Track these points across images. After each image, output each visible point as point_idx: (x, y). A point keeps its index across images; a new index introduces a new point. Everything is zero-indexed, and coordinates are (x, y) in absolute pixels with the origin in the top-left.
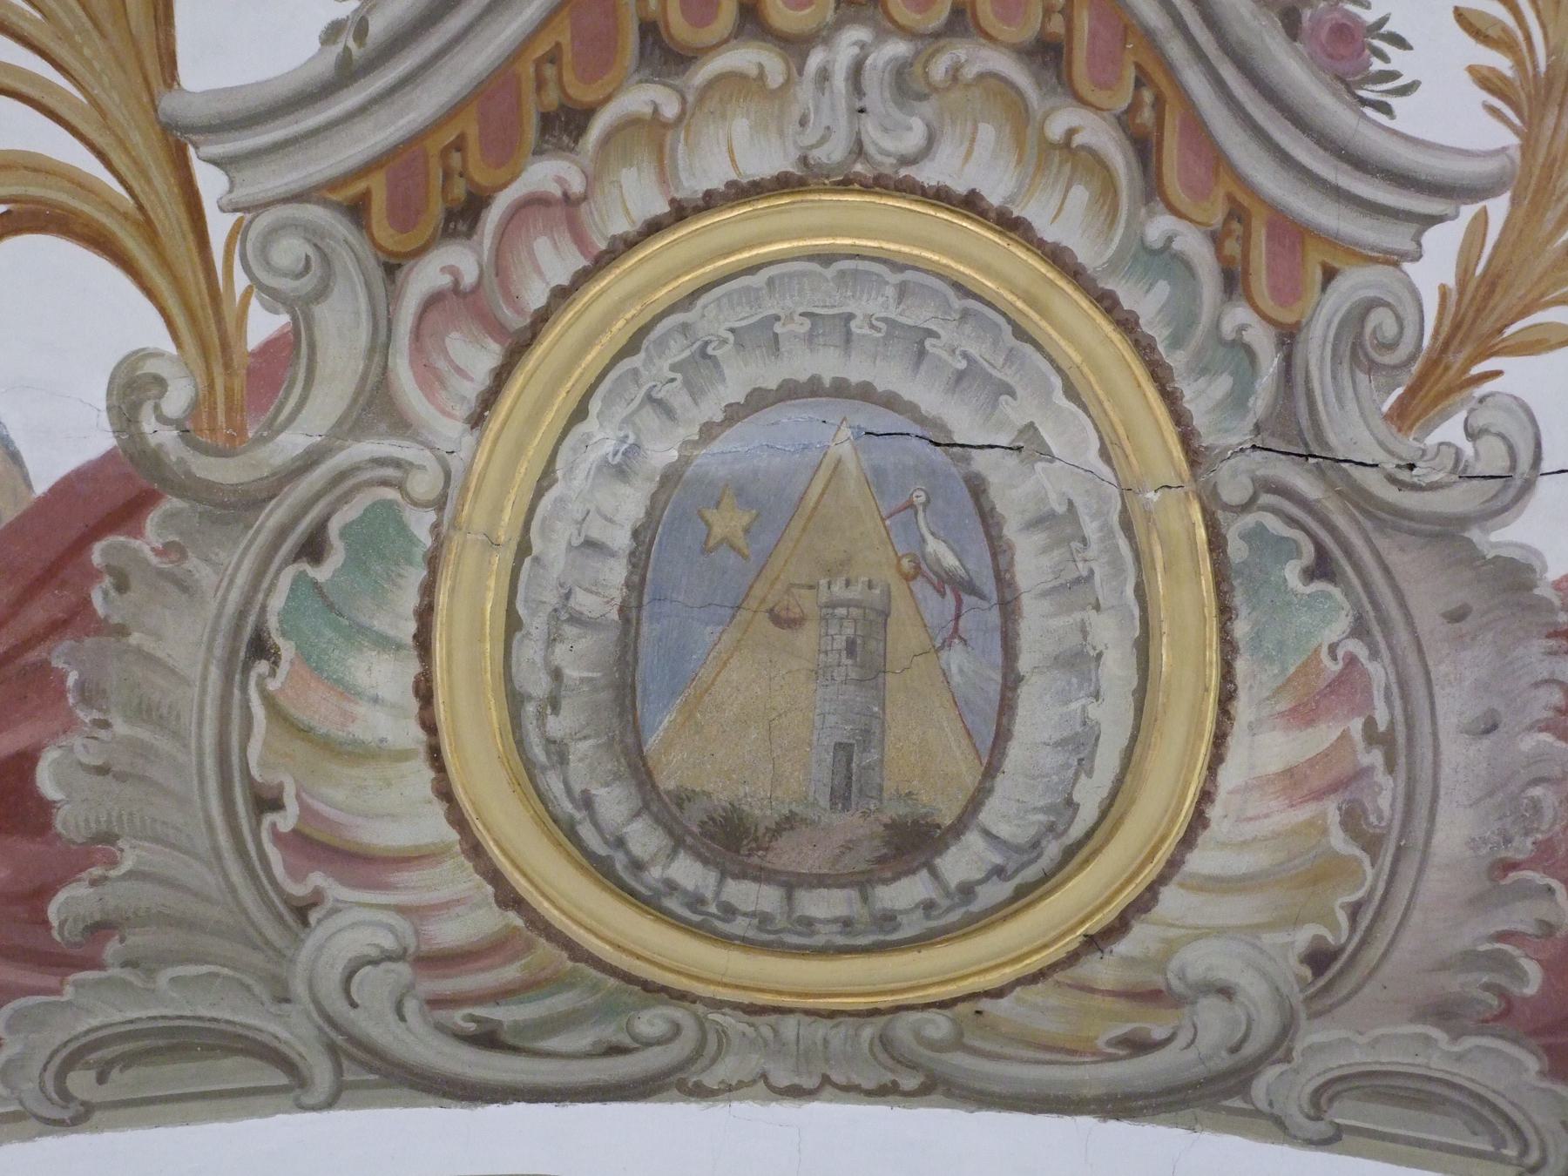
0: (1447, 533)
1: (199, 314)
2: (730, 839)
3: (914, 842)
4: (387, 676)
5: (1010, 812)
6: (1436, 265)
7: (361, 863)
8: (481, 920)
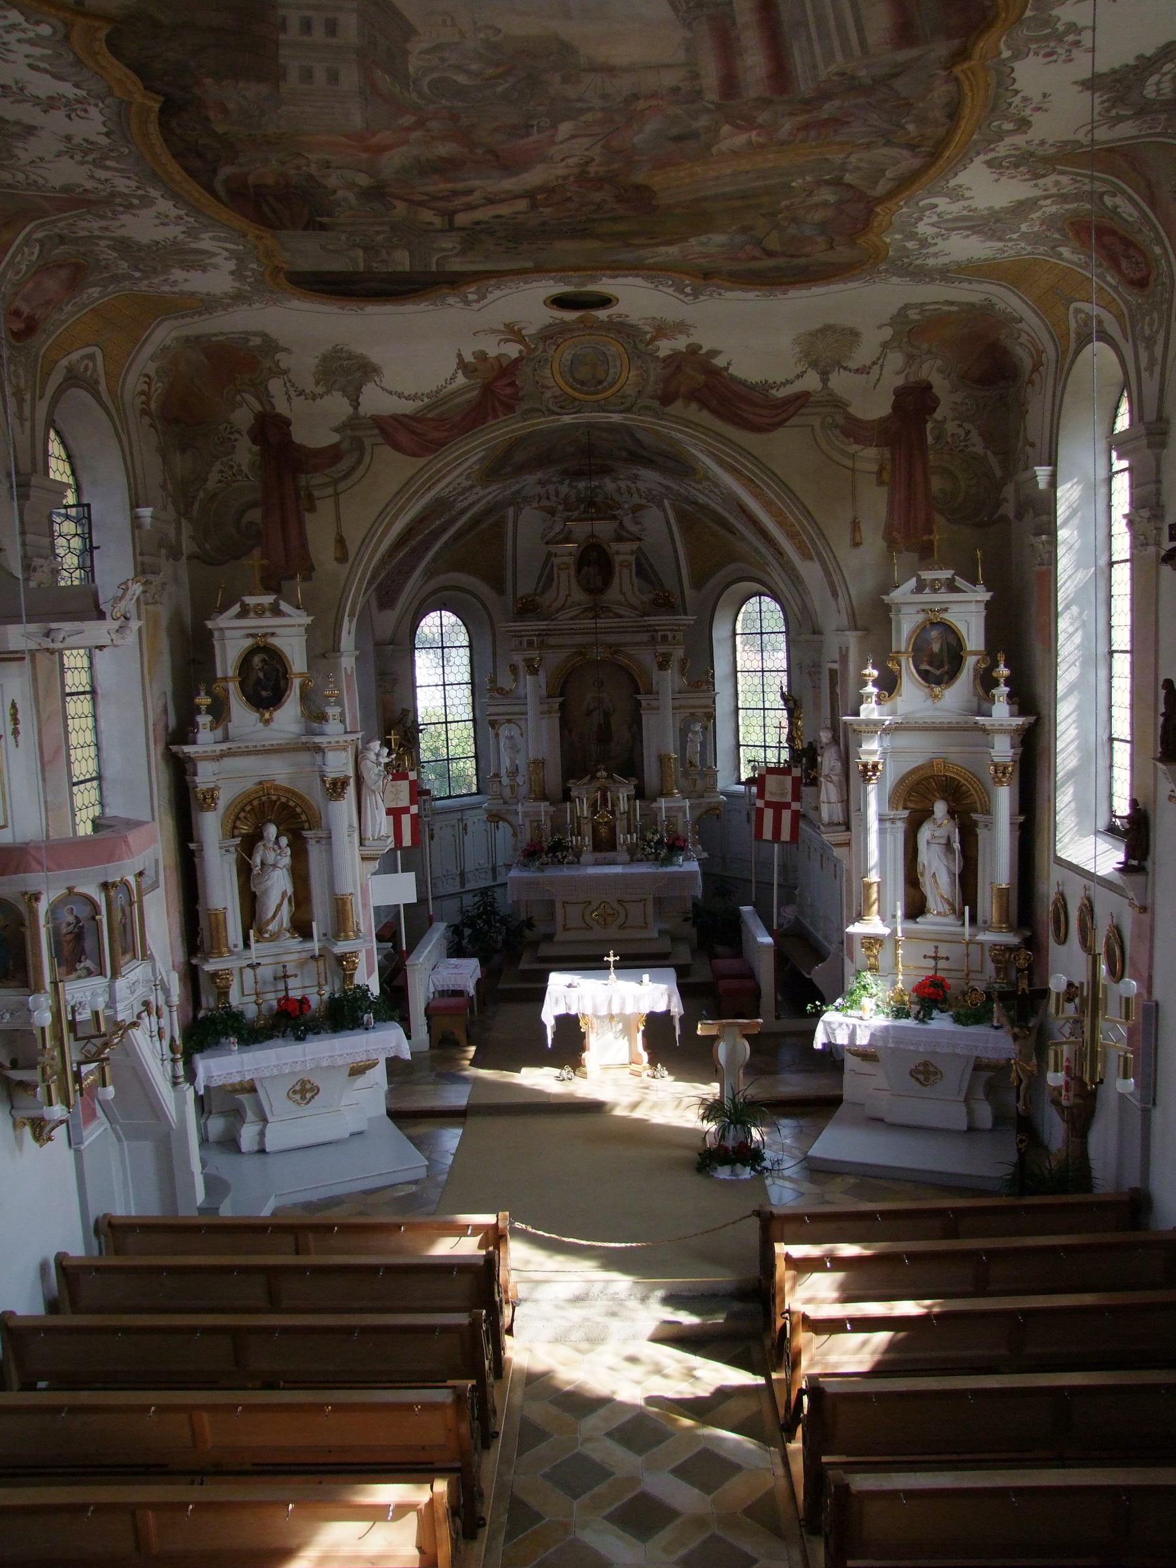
0: (651, 355)
1: (526, 346)
2: (582, 383)
3: (600, 382)
4: (548, 372)
5: (609, 379)
6: (649, 336)
7: (548, 388)
8: (559, 393)
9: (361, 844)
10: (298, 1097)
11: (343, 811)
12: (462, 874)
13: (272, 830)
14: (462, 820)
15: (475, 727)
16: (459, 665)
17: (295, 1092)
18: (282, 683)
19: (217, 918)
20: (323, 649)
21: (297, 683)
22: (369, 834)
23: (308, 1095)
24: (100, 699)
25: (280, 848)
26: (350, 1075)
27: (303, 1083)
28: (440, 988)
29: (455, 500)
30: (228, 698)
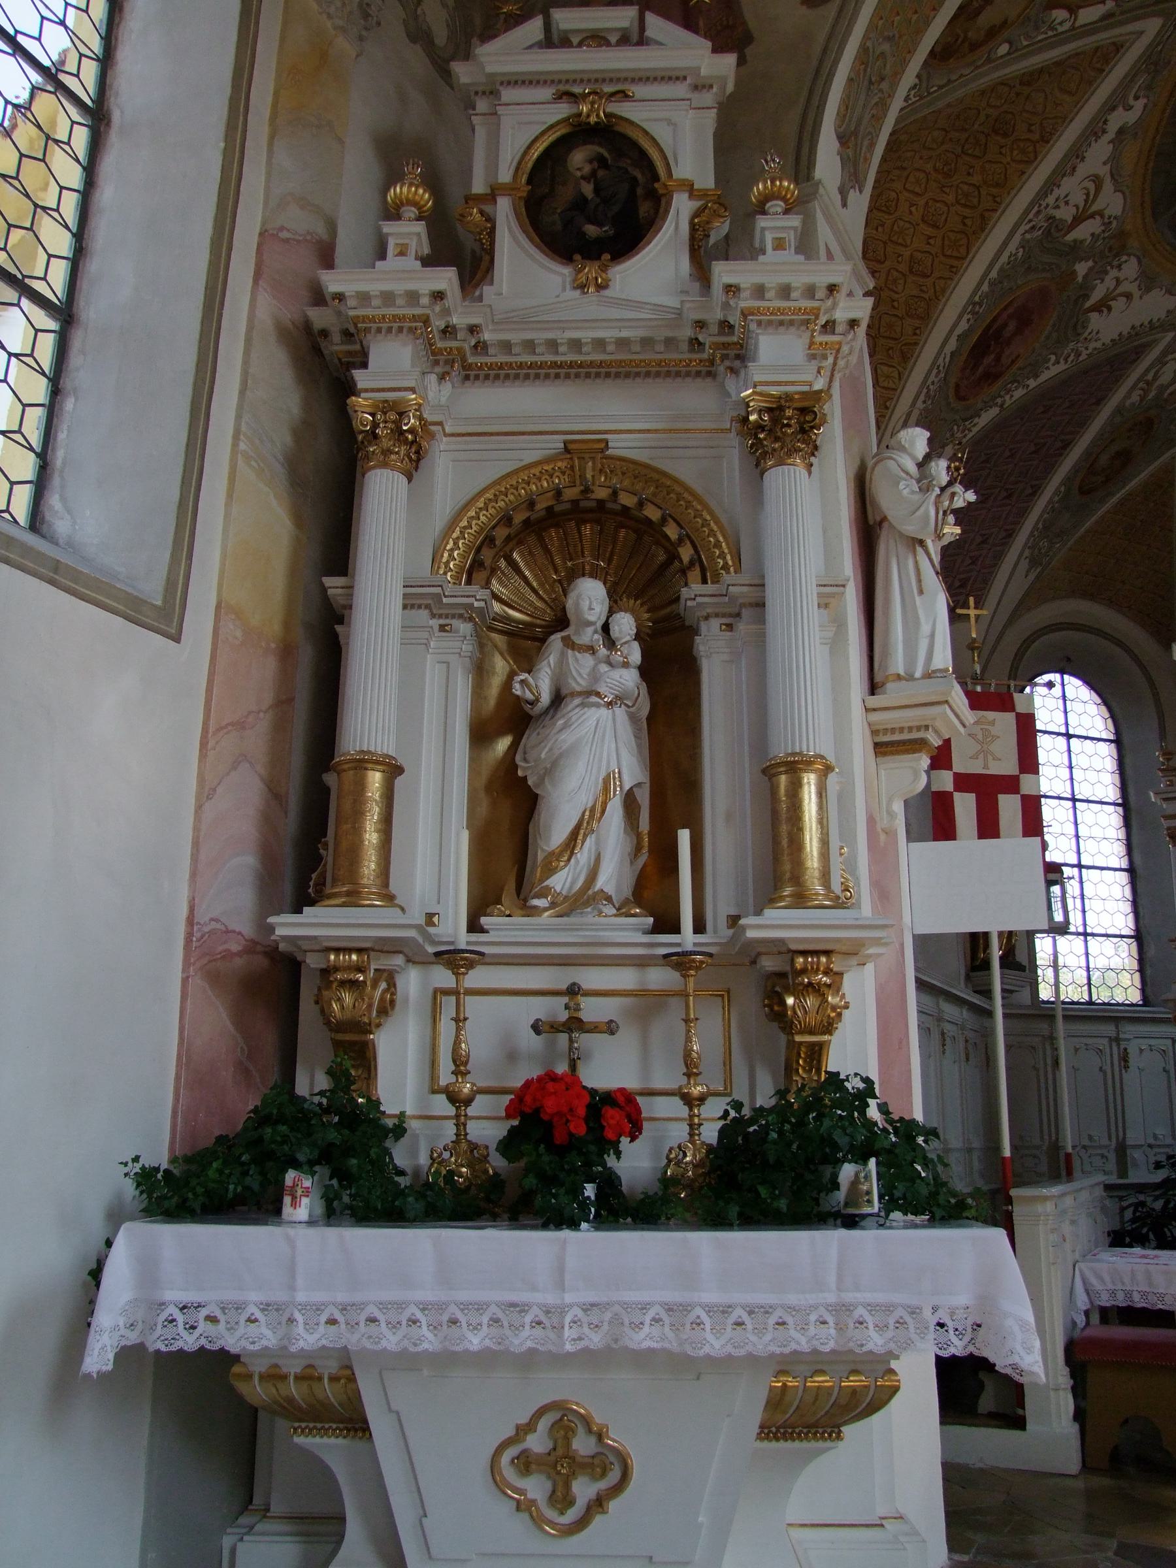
9: (873, 688)
10: (536, 1487)
11: (804, 518)
12: (1122, 1150)
13: (590, 596)
14: (1117, 1040)
15: (1133, 883)
16: (1098, 772)
17: (525, 1463)
18: (644, 209)
19: (361, 786)
20: (761, 132)
21: (682, 208)
22: (898, 664)
23: (584, 1489)
24: (114, 142)
25: (611, 643)
26: (768, 1431)
27: (565, 1420)
28: (1105, 1301)
29: (1085, 290)
30: (492, 232)
